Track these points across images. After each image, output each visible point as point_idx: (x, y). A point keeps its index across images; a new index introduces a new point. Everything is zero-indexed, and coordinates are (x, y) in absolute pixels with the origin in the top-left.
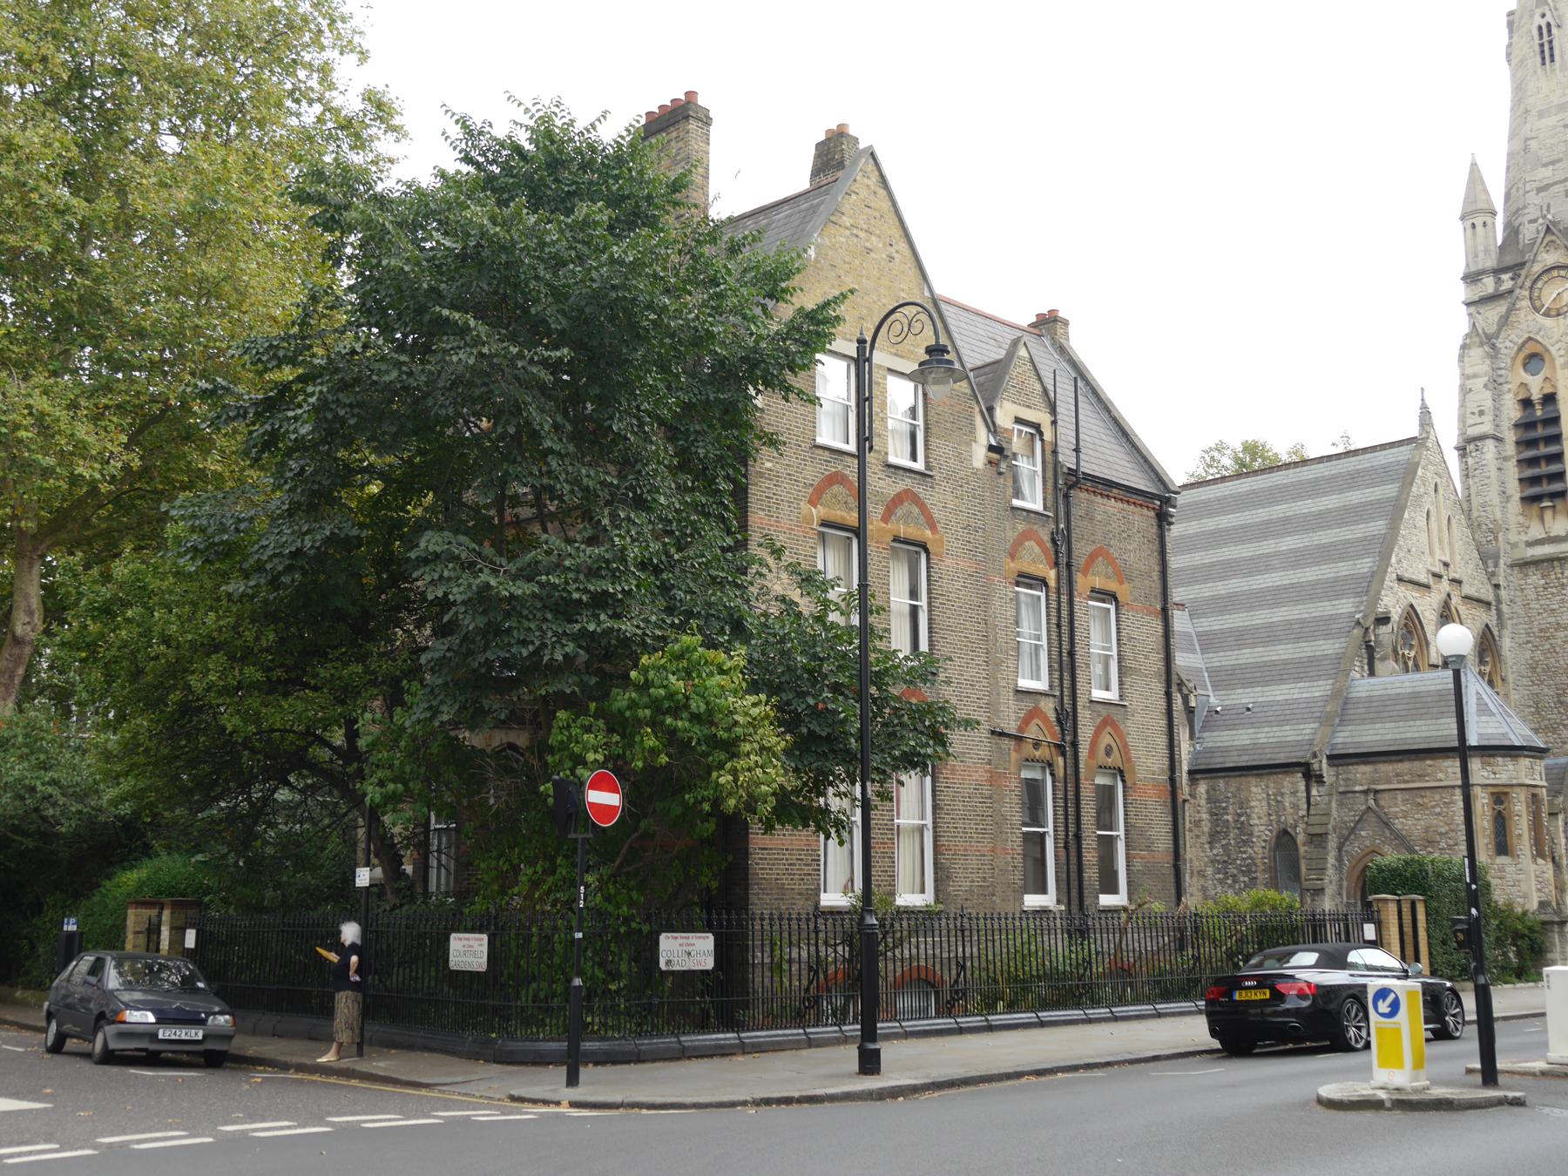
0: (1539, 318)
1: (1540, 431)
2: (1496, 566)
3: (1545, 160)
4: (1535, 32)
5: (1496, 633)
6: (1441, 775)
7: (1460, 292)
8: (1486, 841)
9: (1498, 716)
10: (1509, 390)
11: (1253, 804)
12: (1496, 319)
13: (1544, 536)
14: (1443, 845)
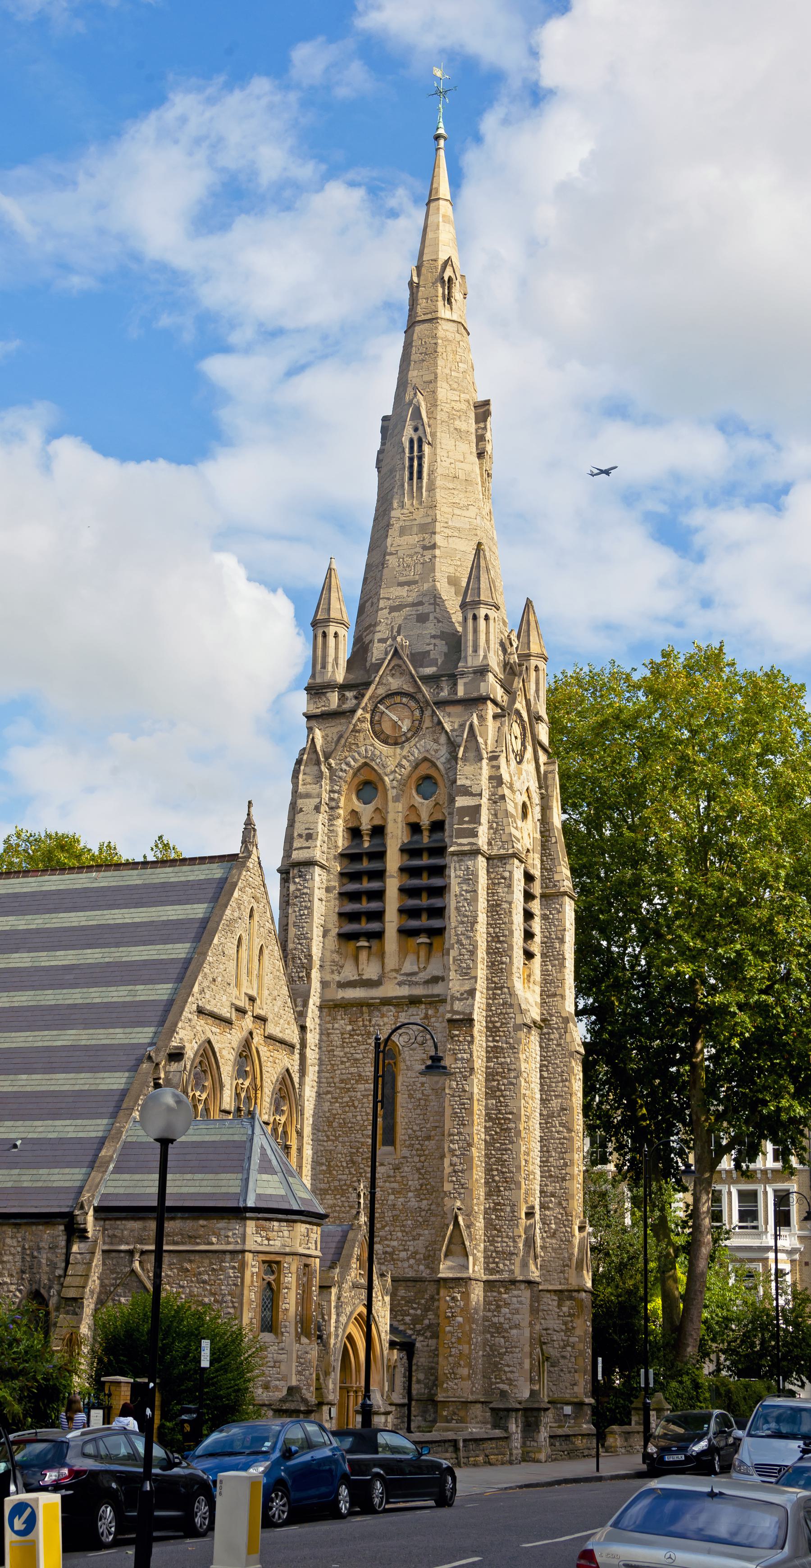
1: (365, 865)
3: (402, 579)
4: (407, 445)
5: (296, 1080)
6: (214, 1240)
9: (280, 1174)
11: (5, 1258)
13: (356, 977)
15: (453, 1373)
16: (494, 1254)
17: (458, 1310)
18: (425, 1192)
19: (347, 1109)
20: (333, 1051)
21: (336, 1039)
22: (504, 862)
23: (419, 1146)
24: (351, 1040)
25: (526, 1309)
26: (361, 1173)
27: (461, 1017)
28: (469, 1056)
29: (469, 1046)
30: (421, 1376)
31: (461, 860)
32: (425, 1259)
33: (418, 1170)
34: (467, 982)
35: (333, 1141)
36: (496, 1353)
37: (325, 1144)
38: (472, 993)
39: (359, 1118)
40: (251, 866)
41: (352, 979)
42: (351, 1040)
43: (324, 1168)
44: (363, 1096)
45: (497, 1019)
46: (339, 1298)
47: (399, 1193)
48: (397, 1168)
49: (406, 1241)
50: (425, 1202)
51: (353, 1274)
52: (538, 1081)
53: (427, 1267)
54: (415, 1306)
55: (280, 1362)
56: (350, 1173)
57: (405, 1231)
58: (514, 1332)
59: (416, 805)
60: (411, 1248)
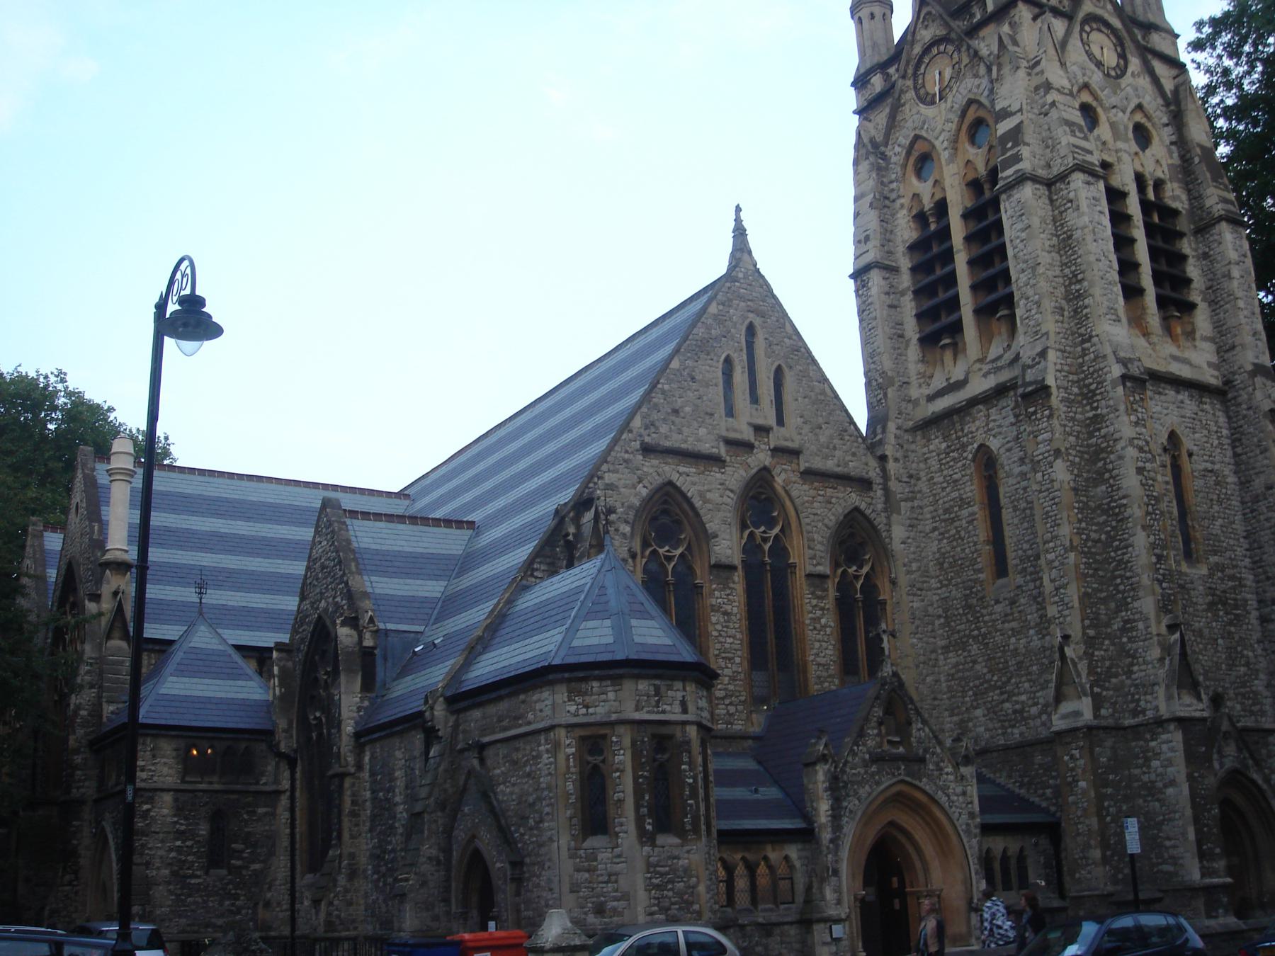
0: (923, 108)
2: (884, 431)
5: (880, 521)
7: (850, 99)
8: (569, 812)
10: (902, 206)
13: (945, 384)
14: (531, 821)
15: (1085, 857)
17: (1080, 771)
19: (955, 543)
20: (932, 478)
21: (934, 463)
23: (1032, 569)
25: (1179, 757)
26: (978, 618)
29: (1048, 421)
31: (1009, 197)
33: (1035, 598)
35: (946, 586)
36: (1152, 823)
37: (939, 591)
38: (1043, 354)
39: (967, 551)
40: (741, 275)
45: (1091, 380)
47: (1019, 632)
48: (1013, 602)
49: (1035, 693)
51: (870, 743)
52: (1232, 461)
55: (616, 874)
56: (968, 621)
58: (1170, 791)
59: (971, 158)
60: (1041, 701)
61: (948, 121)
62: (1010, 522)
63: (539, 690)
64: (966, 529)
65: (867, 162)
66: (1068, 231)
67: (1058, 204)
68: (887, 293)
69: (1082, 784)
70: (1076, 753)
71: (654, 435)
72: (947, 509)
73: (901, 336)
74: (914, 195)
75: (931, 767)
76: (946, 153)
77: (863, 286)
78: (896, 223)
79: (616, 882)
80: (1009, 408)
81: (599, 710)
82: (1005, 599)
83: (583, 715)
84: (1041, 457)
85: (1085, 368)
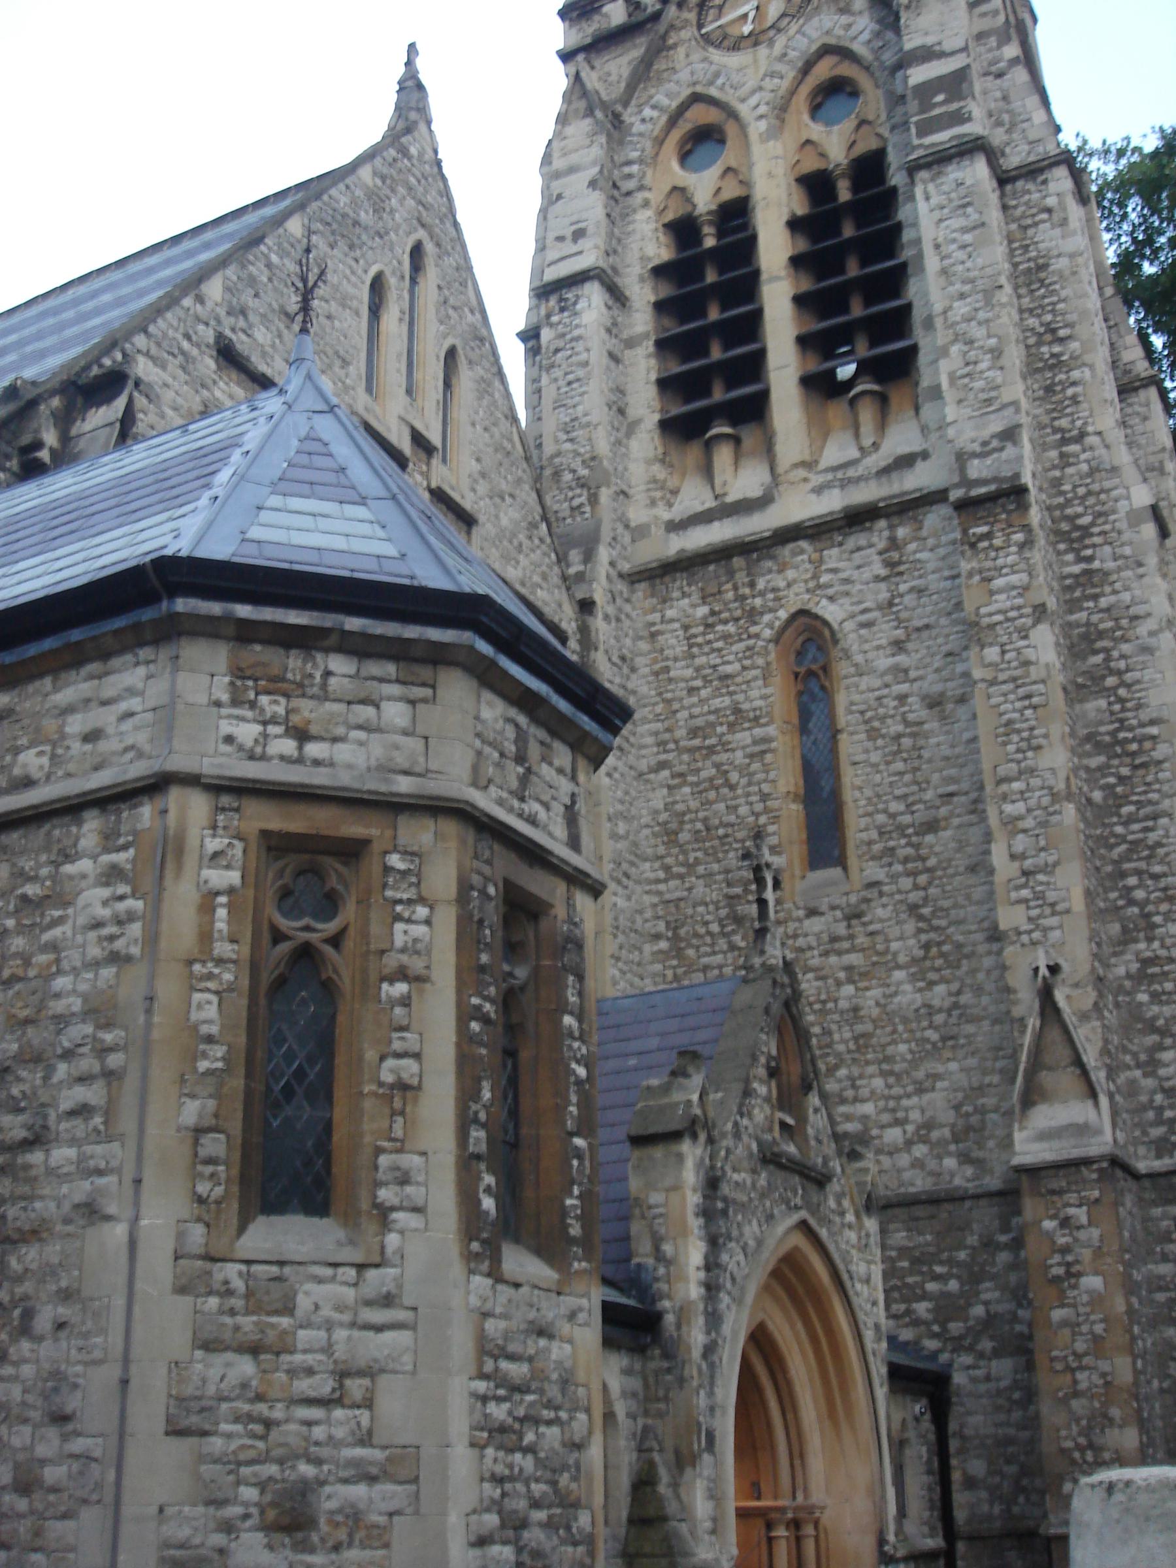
0: (715, 55)
2: (589, 556)
6: (32, 761)
8: (192, 1111)
10: (646, 204)
12: (626, 72)
13: (710, 503)
15: (1091, 1446)
16: (1159, 1098)
17: (1086, 1254)
18: (939, 962)
19: (712, 795)
20: (667, 669)
21: (673, 641)
22: (1041, 178)
23: (910, 851)
24: (711, 637)
27: (993, 487)
28: (1024, 577)
30: (977, 1467)
32: (956, 1139)
33: (913, 909)
34: (992, 417)
35: (681, 877)
37: (662, 887)
39: (743, 810)
41: (700, 508)
42: (711, 637)
43: (663, 945)
44: (752, 756)
45: (1080, 509)
46: (712, 1184)
47: (864, 975)
49: (898, 1098)
50: (940, 989)
53: (965, 1158)
54: (939, 1269)
55: (370, 1372)
56: (733, 947)
57: (891, 1073)
60: (915, 1115)
61: (772, 75)
62: (857, 758)
63: (94, 667)
64: (743, 770)
65: (588, 121)
66: (1037, 257)
67: (1018, 212)
68: (609, 331)
69: (1093, 1282)
70: (1081, 1214)
71: (243, 337)
72: (698, 728)
73: (621, 412)
74: (675, 188)
75: (832, 1203)
76: (763, 125)
77: (562, 310)
78: (630, 228)
79: (368, 1403)
80: (872, 550)
81: (343, 753)
82: (833, 908)
83: (282, 758)
84: (998, 618)
85: (1067, 487)
